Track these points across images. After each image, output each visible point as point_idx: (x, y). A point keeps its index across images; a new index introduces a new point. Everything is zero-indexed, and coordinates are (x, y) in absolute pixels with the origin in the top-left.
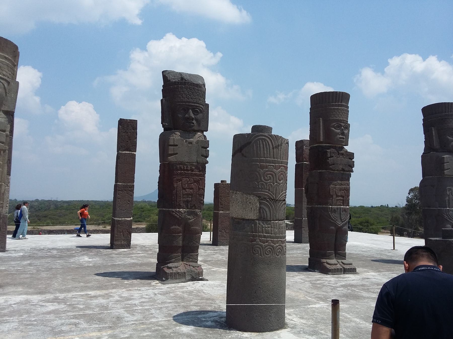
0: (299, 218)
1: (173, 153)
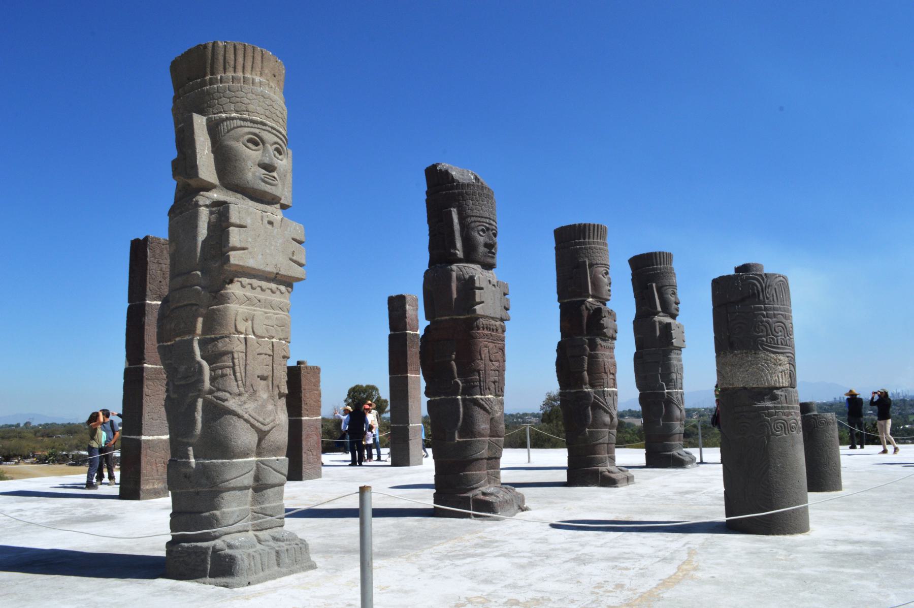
1: (480, 301)
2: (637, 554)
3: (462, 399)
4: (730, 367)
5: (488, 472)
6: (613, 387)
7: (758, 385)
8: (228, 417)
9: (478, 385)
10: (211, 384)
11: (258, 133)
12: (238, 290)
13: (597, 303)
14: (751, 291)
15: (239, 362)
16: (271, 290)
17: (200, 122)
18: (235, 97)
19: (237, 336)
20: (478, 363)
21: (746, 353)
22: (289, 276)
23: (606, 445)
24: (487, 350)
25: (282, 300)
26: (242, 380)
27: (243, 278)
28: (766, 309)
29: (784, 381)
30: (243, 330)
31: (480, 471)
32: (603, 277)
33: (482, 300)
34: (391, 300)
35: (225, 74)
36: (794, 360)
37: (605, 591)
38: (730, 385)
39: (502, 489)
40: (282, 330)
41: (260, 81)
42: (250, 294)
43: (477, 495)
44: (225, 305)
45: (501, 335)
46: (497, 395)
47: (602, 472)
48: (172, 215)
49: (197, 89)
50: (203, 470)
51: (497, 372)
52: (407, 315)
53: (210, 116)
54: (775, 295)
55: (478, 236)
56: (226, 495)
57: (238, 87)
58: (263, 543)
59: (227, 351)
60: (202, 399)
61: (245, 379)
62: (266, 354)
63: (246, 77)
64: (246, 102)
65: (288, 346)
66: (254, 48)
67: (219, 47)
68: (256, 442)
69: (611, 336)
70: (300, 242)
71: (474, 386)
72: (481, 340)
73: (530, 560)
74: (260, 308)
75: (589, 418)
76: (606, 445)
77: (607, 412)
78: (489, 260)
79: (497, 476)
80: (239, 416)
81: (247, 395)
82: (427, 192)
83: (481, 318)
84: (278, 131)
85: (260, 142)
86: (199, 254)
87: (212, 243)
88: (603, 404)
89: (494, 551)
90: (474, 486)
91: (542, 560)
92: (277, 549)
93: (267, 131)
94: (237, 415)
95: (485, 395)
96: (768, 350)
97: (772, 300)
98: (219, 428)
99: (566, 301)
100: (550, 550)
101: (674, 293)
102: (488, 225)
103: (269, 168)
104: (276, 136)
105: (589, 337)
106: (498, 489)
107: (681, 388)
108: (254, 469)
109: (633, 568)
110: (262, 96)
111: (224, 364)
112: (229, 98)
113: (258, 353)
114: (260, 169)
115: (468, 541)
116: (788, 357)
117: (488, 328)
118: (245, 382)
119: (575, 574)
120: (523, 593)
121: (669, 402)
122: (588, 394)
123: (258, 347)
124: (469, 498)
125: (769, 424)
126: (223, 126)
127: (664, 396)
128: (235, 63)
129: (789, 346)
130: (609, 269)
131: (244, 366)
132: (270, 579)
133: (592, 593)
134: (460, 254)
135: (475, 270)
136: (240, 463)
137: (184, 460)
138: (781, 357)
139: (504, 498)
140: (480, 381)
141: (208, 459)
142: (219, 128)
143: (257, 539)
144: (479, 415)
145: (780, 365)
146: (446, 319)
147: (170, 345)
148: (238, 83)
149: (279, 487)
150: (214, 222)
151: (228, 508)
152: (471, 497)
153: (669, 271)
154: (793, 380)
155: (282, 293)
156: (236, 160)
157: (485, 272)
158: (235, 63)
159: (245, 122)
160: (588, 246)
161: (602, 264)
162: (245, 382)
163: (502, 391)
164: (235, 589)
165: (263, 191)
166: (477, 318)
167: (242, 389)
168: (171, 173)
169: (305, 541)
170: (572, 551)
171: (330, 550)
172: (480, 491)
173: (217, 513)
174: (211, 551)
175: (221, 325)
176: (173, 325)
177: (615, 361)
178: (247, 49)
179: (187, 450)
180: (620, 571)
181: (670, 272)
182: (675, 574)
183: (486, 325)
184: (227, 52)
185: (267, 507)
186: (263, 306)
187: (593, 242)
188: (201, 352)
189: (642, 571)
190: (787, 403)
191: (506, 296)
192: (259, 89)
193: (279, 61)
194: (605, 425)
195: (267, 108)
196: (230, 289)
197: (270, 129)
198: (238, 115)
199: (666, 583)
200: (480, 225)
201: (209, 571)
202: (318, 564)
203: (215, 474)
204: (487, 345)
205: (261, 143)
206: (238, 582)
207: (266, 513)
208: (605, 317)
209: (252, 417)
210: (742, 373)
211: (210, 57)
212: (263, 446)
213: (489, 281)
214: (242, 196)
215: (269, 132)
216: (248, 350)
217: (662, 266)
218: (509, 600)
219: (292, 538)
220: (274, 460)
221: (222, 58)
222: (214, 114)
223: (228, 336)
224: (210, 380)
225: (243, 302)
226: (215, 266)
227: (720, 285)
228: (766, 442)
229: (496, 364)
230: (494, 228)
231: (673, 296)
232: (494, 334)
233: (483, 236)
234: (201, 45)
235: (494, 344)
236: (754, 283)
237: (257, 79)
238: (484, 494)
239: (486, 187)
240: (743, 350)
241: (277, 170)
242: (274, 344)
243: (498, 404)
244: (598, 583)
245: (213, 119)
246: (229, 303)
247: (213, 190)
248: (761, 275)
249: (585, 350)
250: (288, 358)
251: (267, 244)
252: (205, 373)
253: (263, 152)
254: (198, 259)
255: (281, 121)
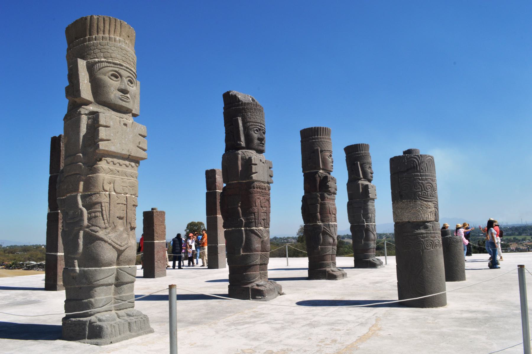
0: (213, 245)
2: (346, 321)
3: (244, 230)
4: (400, 210)
5: (260, 272)
6: (334, 222)
7: (417, 220)
8: (98, 242)
9: (254, 221)
10: (88, 222)
11: (118, 70)
12: (105, 165)
13: (325, 173)
14: (412, 165)
15: (105, 209)
16: (126, 165)
17: (82, 64)
18: (104, 49)
19: (104, 193)
20: (254, 208)
21: (410, 201)
22: (137, 157)
23: (330, 255)
24: (260, 201)
25: (132, 171)
26: (107, 219)
27: (108, 158)
28: (421, 175)
29: (432, 217)
30: (108, 189)
31: (255, 272)
32: (329, 158)
33: (256, 171)
34: (207, 172)
35: (98, 35)
36: (438, 205)
37: (325, 345)
38: (400, 220)
39: (269, 283)
40: (133, 189)
41: (119, 39)
42: (112, 167)
43: (254, 286)
44: (97, 174)
45: (268, 192)
46: (265, 227)
47: (328, 271)
48: (66, 120)
49: (81, 44)
50: (84, 275)
51: (265, 214)
52: (217, 181)
53: (89, 60)
54: (426, 167)
55: (254, 133)
56: (98, 289)
57: (105, 42)
58: (121, 318)
59: (98, 202)
60: (83, 231)
61: (109, 219)
62: (122, 204)
63: (111, 37)
64: (110, 52)
65: (136, 199)
66: (115, 19)
67: (94, 19)
68: (116, 256)
69: (333, 192)
70: (144, 137)
71: (252, 222)
72: (255, 195)
73: (282, 325)
74: (119, 176)
75: (321, 240)
76: (330, 255)
77: (331, 236)
78: (261, 148)
79: (265, 275)
80: (105, 241)
81: (110, 229)
82: (224, 108)
83: (256, 182)
85: (119, 76)
86: (81, 144)
87: (89, 137)
88: (329, 232)
89: (262, 320)
90: (252, 281)
91: (289, 325)
92: (129, 321)
93: (123, 69)
94: (104, 241)
95: (258, 227)
96: (422, 200)
97: (424, 170)
98: (93, 248)
99: (307, 172)
100: (295, 319)
101: (370, 168)
102: (259, 127)
103: (124, 91)
104: (129, 72)
105: (320, 193)
106: (266, 282)
107: (374, 222)
108: (115, 273)
109: (343, 330)
110: (120, 48)
111: (96, 210)
112: (100, 49)
113: (118, 203)
114: (119, 92)
115: (247, 314)
116: (434, 203)
117: (260, 188)
118: (109, 220)
119: (308, 334)
120: (276, 346)
121: (367, 230)
122: (320, 226)
123: (118, 200)
124: (249, 288)
125: (423, 243)
126: (96, 66)
127: (365, 227)
128: (104, 28)
129: (435, 197)
130: (332, 153)
131: (108, 211)
132: (124, 339)
133: (318, 346)
134: (243, 144)
135: (252, 154)
136: (106, 269)
137: (72, 268)
138: (430, 204)
139: (269, 288)
140: (255, 219)
141: (86, 268)
142: (94, 67)
143: (117, 315)
144: (255, 239)
145: (429, 208)
146: (235, 183)
147: (64, 199)
148: (106, 41)
149: (131, 284)
150: (90, 124)
151: (99, 297)
152: (250, 287)
153: (367, 155)
154: (437, 217)
155: (132, 167)
156: (104, 87)
157: (258, 155)
158: (104, 28)
159: (110, 64)
160: (320, 140)
161: (328, 151)
162: (109, 220)
163: (269, 225)
164: (102, 346)
165: (120, 105)
166: (253, 182)
167: (107, 225)
168: (65, 94)
169: (147, 316)
170: (308, 319)
171: (164, 320)
172: (255, 283)
173: (92, 300)
174: (88, 323)
175: (94, 186)
176: (65, 187)
177: (336, 207)
178: (111, 20)
179: (74, 262)
180: (335, 332)
181: (367, 156)
182: (367, 333)
183: (259, 186)
184: (99, 22)
185: (123, 296)
186: (121, 175)
187: (323, 137)
188: (82, 202)
189: (348, 331)
190: (433, 230)
191: (271, 169)
192: (119, 44)
193: (132, 28)
194: (330, 244)
195: (123, 55)
196: (100, 164)
197: (125, 68)
198: (105, 60)
199: (362, 339)
200: (255, 127)
201: (87, 335)
202: (155, 330)
203: (91, 277)
204: (259, 198)
205: (119, 77)
206: (104, 342)
207: (123, 299)
208: (330, 181)
209: (114, 242)
210: (407, 213)
211: (89, 25)
212: (121, 259)
213: (261, 160)
214: (108, 108)
215: (125, 70)
216: (111, 201)
217: (363, 152)
218: (267, 351)
219: (139, 314)
220: (128, 267)
221: (96, 25)
222: (91, 59)
223: (98, 192)
224: (88, 219)
225: (108, 172)
226: (91, 150)
227: (394, 162)
228: (422, 253)
229: (265, 209)
230: (263, 129)
231: (369, 169)
232: (263, 191)
233: (257, 134)
234: (83, 18)
235: (263, 197)
236: (413, 160)
237: (118, 38)
238: (258, 285)
239: (259, 105)
240: (408, 200)
241: (129, 93)
242: (128, 198)
243: (266, 232)
244: (321, 339)
245: (90, 62)
246: (99, 173)
247: (90, 105)
248: (418, 156)
249: (318, 200)
250: (137, 206)
251: (123, 137)
252: (84, 215)
253: (121, 82)
254: (80, 146)
255: (132, 64)
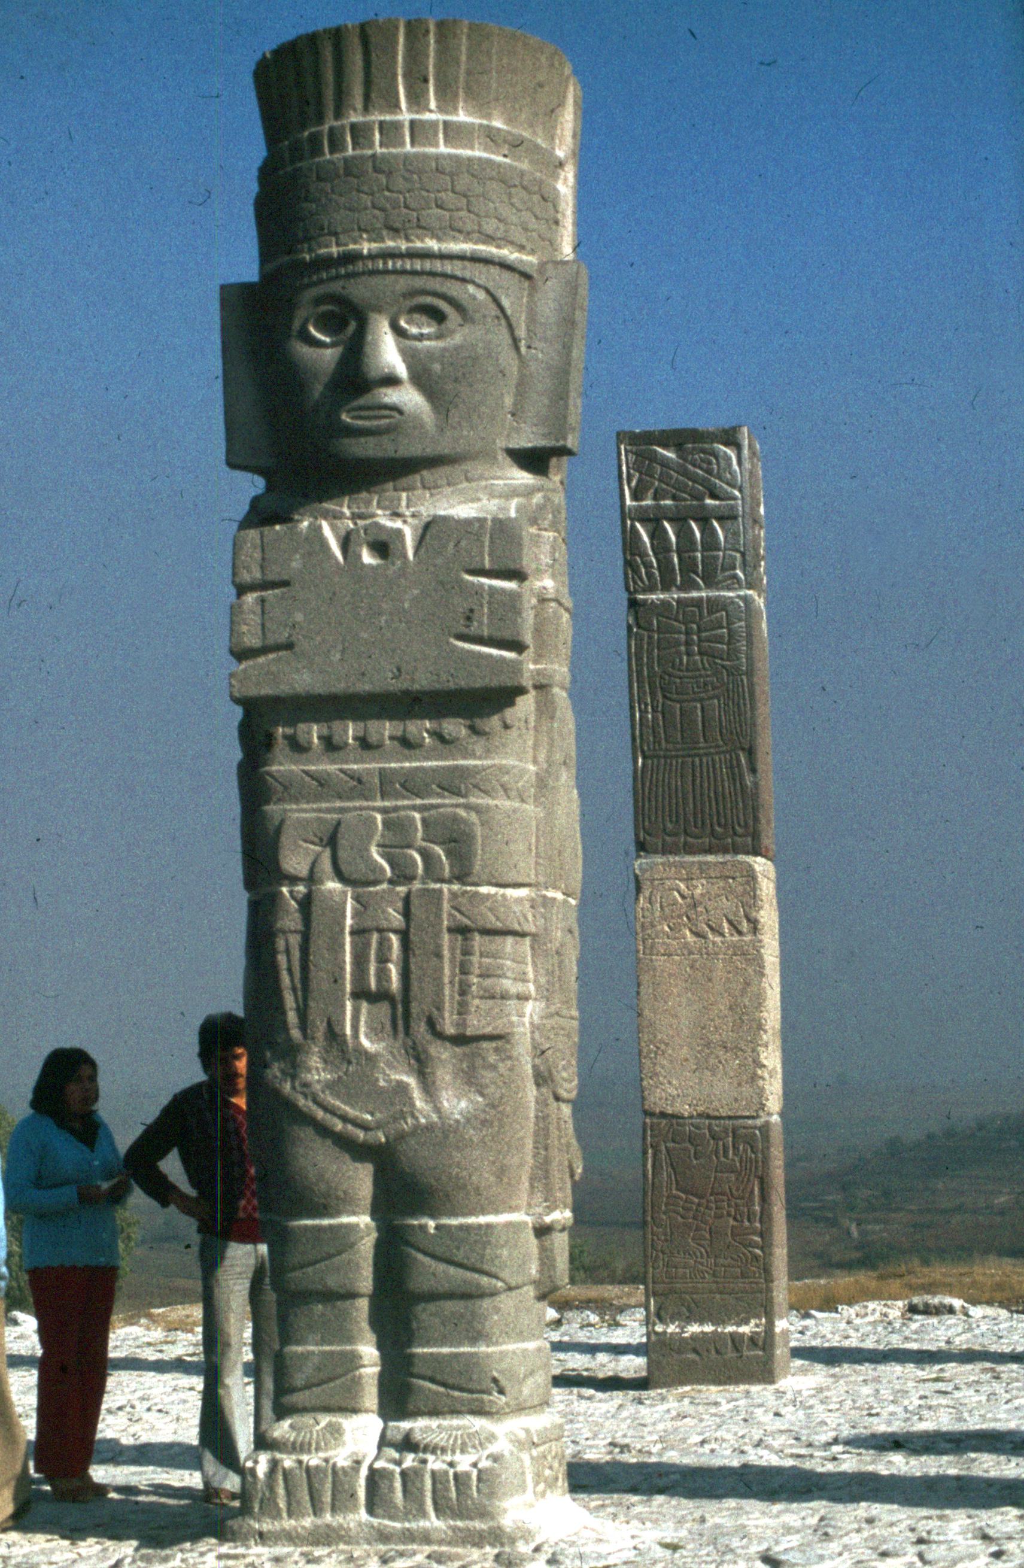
84: (412, 255)
215: (375, 272)
